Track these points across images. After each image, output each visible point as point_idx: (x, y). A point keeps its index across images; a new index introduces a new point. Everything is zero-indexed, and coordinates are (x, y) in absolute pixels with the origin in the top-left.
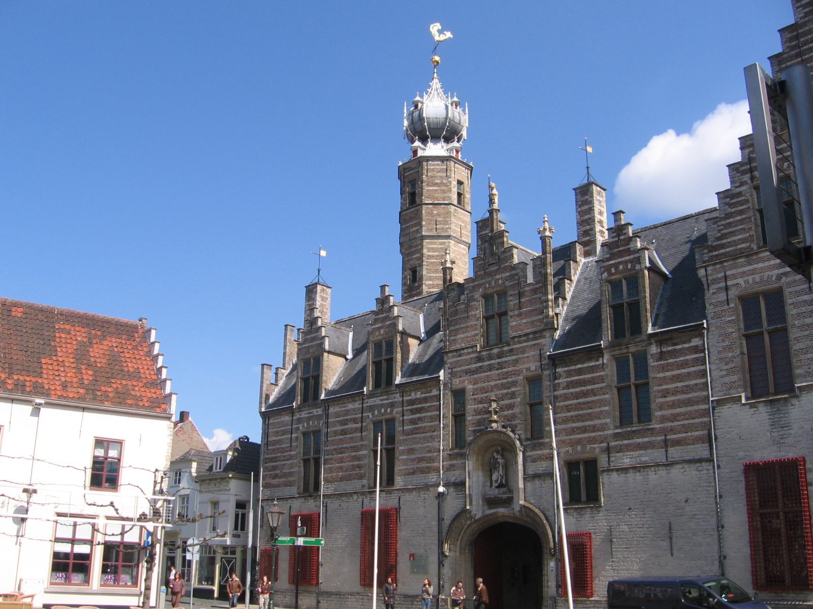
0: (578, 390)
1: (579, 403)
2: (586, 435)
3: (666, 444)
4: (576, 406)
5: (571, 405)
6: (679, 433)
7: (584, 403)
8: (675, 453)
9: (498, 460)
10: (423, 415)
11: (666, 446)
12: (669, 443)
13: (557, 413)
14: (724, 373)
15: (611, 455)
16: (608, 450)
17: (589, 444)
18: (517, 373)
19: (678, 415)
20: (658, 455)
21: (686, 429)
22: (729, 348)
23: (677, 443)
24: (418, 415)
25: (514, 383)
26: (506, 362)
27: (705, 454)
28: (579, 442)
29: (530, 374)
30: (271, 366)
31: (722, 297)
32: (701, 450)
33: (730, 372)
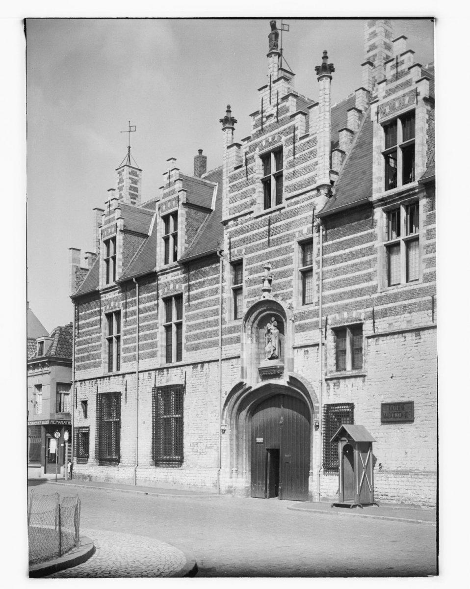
0: (347, 251)
1: (347, 266)
4: (344, 269)
7: (353, 265)
9: (271, 331)
13: (326, 278)
15: (376, 321)
16: (373, 316)
17: (355, 310)
18: (289, 238)
24: (201, 290)
26: (280, 227)
28: (346, 307)
29: (302, 238)
30: (80, 250)
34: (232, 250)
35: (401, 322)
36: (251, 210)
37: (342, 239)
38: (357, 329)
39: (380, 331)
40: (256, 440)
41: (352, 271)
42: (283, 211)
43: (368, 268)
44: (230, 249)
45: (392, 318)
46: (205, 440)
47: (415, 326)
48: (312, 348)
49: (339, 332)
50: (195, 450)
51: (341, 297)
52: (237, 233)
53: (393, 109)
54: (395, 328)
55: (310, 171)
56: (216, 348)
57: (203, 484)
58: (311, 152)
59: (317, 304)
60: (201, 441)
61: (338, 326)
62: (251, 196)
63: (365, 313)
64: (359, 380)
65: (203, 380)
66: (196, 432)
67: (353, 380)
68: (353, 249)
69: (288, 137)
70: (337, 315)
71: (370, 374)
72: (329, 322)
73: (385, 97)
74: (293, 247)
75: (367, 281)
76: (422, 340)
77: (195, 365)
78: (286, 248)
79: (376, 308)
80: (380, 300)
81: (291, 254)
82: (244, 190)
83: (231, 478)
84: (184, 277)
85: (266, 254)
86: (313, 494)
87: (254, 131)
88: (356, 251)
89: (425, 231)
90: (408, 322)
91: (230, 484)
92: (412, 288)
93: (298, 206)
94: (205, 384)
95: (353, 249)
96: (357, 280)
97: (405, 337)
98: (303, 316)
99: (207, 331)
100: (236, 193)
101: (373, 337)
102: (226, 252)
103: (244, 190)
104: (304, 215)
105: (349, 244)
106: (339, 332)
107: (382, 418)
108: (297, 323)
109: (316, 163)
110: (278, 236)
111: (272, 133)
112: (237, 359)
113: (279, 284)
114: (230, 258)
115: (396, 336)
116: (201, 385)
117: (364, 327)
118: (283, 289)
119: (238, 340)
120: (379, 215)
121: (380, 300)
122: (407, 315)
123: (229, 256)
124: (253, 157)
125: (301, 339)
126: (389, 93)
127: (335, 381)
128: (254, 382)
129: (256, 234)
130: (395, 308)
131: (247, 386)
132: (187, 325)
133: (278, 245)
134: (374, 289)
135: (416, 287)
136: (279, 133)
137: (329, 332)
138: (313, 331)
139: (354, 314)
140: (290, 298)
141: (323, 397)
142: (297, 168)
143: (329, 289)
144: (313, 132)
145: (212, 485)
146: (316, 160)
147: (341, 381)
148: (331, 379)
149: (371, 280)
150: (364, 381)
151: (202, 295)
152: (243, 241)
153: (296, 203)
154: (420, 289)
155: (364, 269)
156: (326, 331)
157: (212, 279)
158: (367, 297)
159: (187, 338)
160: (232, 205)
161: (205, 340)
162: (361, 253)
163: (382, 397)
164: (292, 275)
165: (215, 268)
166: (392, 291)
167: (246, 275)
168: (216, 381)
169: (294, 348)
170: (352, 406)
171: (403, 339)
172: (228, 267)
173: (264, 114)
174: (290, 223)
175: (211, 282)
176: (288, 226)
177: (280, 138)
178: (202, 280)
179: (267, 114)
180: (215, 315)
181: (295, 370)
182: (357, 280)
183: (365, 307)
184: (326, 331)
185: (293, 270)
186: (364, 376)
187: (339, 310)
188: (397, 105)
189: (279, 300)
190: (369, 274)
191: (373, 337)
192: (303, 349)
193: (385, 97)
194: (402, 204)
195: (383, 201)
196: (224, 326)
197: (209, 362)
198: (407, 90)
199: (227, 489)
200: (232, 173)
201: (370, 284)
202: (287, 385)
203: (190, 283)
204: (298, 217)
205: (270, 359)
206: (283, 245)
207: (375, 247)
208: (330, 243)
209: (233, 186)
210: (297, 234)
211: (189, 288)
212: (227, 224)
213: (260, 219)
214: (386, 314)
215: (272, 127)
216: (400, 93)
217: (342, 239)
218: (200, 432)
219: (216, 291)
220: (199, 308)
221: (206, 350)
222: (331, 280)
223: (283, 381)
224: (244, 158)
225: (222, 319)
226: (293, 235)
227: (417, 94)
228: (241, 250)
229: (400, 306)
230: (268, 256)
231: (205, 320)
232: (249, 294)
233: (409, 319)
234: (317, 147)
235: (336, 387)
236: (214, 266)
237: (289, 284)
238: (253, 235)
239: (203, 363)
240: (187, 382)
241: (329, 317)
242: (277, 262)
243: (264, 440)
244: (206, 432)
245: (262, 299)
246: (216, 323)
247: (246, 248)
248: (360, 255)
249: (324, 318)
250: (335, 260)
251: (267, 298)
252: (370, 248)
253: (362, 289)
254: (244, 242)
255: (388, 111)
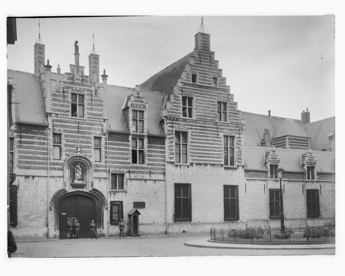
1: (118, 152)
2: (120, 165)
3: (150, 173)
5: (115, 152)
6: (155, 170)
7: (121, 153)
8: (153, 177)
10: (34, 140)
11: (150, 174)
12: (151, 173)
14: (170, 153)
19: (154, 164)
20: (147, 176)
21: (156, 169)
22: (172, 146)
23: (154, 173)
24: (31, 140)
25: (88, 138)
26: (84, 127)
27: (162, 179)
28: (118, 167)
31: (170, 129)
32: (161, 177)
33: (172, 154)
34: (54, 128)
35: (140, 176)
36: (66, 114)
37: (116, 142)
38: (122, 175)
39: (132, 178)
40: (61, 214)
41: (120, 155)
42: (85, 121)
43: (127, 155)
44: (53, 126)
45: (137, 174)
46: (35, 214)
47: (144, 178)
48: (103, 179)
49: (114, 175)
50: (27, 219)
51: (116, 162)
52: (57, 121)
53: (137, 107)
54: (138, 177)
55: (100, 111)
56: (44, 170)
57: (36, 235)
58: (100, 104)
59: (104, 163)
60: (32, 214)
61: (114, 173)
62: (67, 108)
63: (126, 171)
64: (124, 194)
65: (35, 184)
66: (28, 210)
67: (121, 193)
68: (121, 147)
69: (88, 93)
70: (114, 169)
71: (128, 191)
72: (111, 171)
73: (134, 101)
74: (92, 137)
75: (126, 160)
76: (147, 183)
77: (27, 177)
78: (88, 137)
79: (130, 170)
80: (131, 167)
81: (91, 140)
82: (62, 103)
83: (55, 231)
84: (16, 130)
85: (77, 136)
86: (105, 234)
87: (68, 81)
88: (122, 148)
89: (147, 150)
90: (142, 177)
91: (55, 234)
92: (143, 166)
93: (94, 122)
94: (36, 187)
95: (121, 147)
96: (123, 158)
97: (141, 181)
98: (97, 166)
99: (36, 161)
100: (57, 103)
101: (129, 179)
102: (50, 126)
103: (62, 103)
104: (97, 127)
105: (121, 145)
106: (114, 175)
107: (134, 207)
108: (95, 168)
109: (103, 110)
110: (84, 130)
111: (79, 87)
112: (59, 178)
113: (84, 150)
114: (53, 131)
115: (138, 180)
116: (32, 187)
117: (125, 175)
118: (87, 153)
119: (62, 169)
120: (130, 138)
121: (131, 167)
122: (141, 174)
123: (52, 130)
124: (67, 92)
125: (96, 174)
126: (135, 101)
127: (114, 193)
128: (70, 189)
129: (70, 126)
130: (137, 171)
131: (66, 190)
132: (19, 155)
133: (83, 134)
134: (129, 163)
135: (144, 166)
136: (83, 89)
137: (110, 175)
138: (103, 173)
139: (121, 170)
140: (91, 158)
141: (109, 198)
142: (93, 107)
143: (110, 159)
144: (101, 97)
145: (43, 235)
146: (102, 108)
147: (117, 193)
148: (112, 192)
149: (128, 160)
150: (126, 194)
151: (32, 143)
152: (62, 126)
153: (93, 121)
154: (146, 167)
155: (125, 155)
156: (109, 174)
157: (40, 137)
158: (126, 165)
159: (19, 162)
160: (54, 107)
161: (35, 165)
162: (124, 149)
163: (133, 200)
164: (91, 148)
165: (42, 132)
166: (135, 165)
167: (63, 141)
168: (44, 186)
169: (94, 178)
170: (122, 202)
171: (140, 182)
172: (51, 134)
173: (74, 76)
174: (90, 128)
175: (39, 138)
176: (89, 129)
177: (84, 92)
178: (32, 135)
179: (77, 78)
180: (43, 155)
181: (94, 186)
182: (123, 158)
183: (125, 168)
184: (109, 174)
185: (92, 147)
186: (126, 192)
187: (116, 167)
188: (142, 107)
189: (88, 157)
190: (127, 158)
191: (129, 179)
192: (98, 179)
193: (134, 101)
194: (138, 138)
195: (133, 135)
196: (50, 161)
197: (39, 177)
198: (142, 104)
199: (54, 236)
200: (54, 92)
201: (128, 161)
202: (89, 192)
203: (21, 134)
204: (94, 127)
205: (78, 180)
206: (86, 135)
207: (129, 149)
208: (110, 142)
209: (55, 99)
210: (94, 133)
211: (21, 137)
212: (51, 114)
213: (73, 120)
214: (134, 172)
215: (78, 84)
216: (139, 103)
217: (116, 142)
218: (31, 210)
219: (44, 144)
220: (29, 149)
221: (36, 170)
222: (111, 155)
223: (87, 189)
224: (62, 90)
225: (50, 158)
226: (92, 133)
227: (146, 107)
228: (61, 130)
229: (139, 171)
230: (78, 137)
231: (35, 156)
232: (66, 151)
233: (142, 176)
234: (103, 103)
235: (114, 195)
236: (41, 131)
237: (90, 152)
238: (68, 125)
239: (33, 177)
240: (19, 184)
241: (110, 169)
242: (83, 141)
243: (66, 214)
244: (37, 210)
245: (78, 155)
246: (44, 159)
247: (64, 130)
248: (123, 150)
249: (109, 169)
250: (113, 149)
251: (80, 155)
252: (128, 149)
253: (124, 162)
254: (63, 127)
255: (135, 106)
